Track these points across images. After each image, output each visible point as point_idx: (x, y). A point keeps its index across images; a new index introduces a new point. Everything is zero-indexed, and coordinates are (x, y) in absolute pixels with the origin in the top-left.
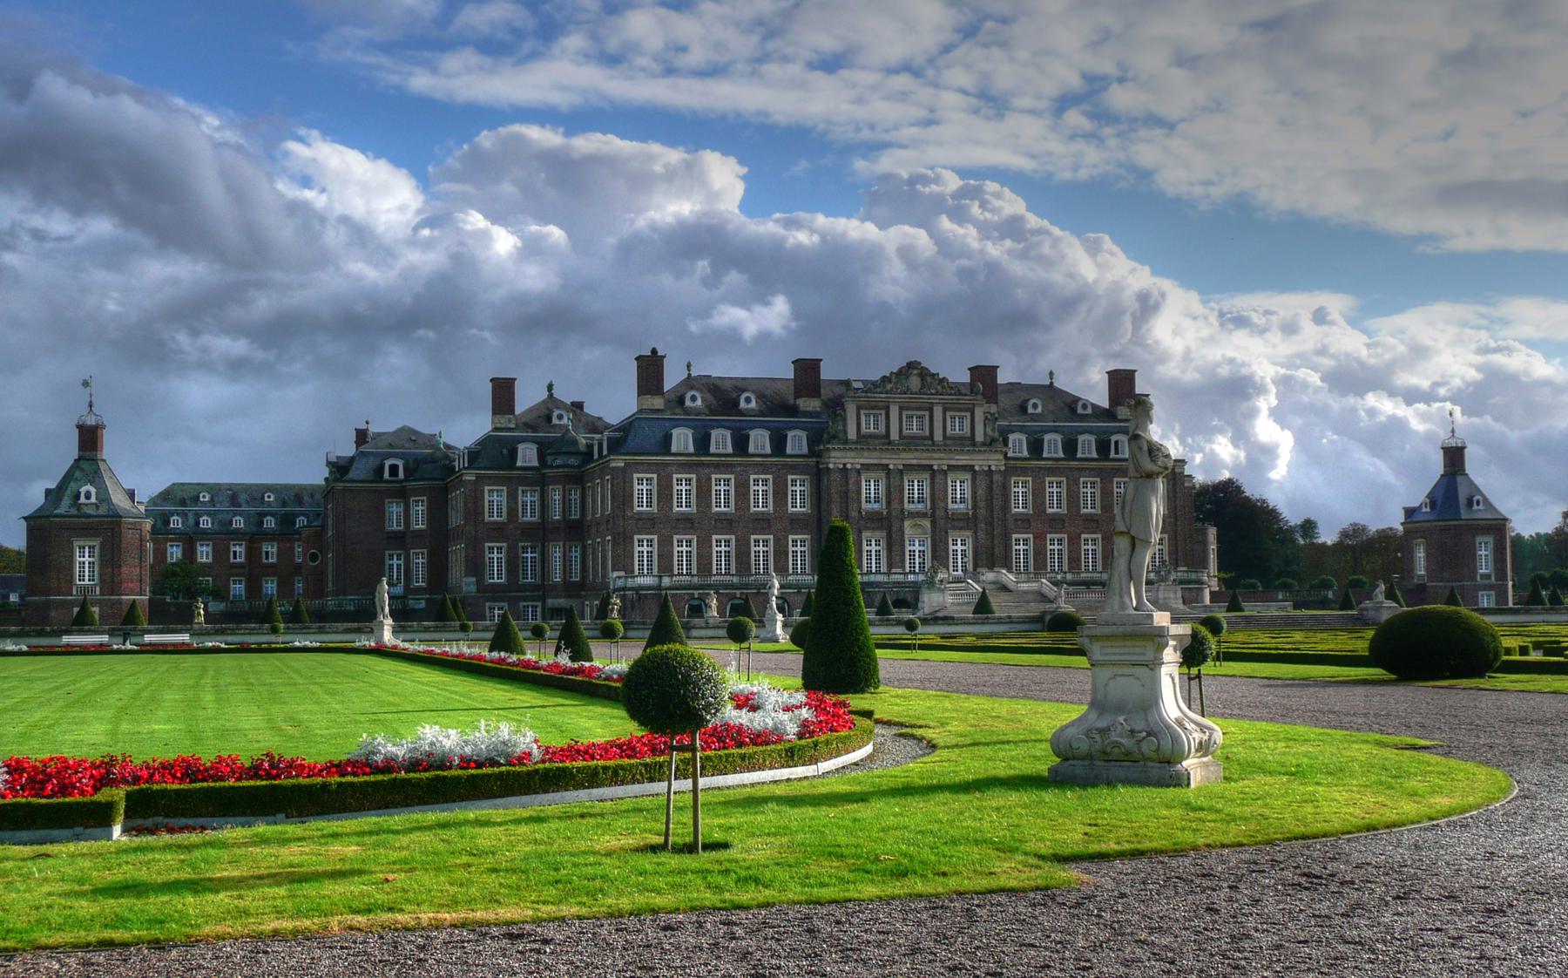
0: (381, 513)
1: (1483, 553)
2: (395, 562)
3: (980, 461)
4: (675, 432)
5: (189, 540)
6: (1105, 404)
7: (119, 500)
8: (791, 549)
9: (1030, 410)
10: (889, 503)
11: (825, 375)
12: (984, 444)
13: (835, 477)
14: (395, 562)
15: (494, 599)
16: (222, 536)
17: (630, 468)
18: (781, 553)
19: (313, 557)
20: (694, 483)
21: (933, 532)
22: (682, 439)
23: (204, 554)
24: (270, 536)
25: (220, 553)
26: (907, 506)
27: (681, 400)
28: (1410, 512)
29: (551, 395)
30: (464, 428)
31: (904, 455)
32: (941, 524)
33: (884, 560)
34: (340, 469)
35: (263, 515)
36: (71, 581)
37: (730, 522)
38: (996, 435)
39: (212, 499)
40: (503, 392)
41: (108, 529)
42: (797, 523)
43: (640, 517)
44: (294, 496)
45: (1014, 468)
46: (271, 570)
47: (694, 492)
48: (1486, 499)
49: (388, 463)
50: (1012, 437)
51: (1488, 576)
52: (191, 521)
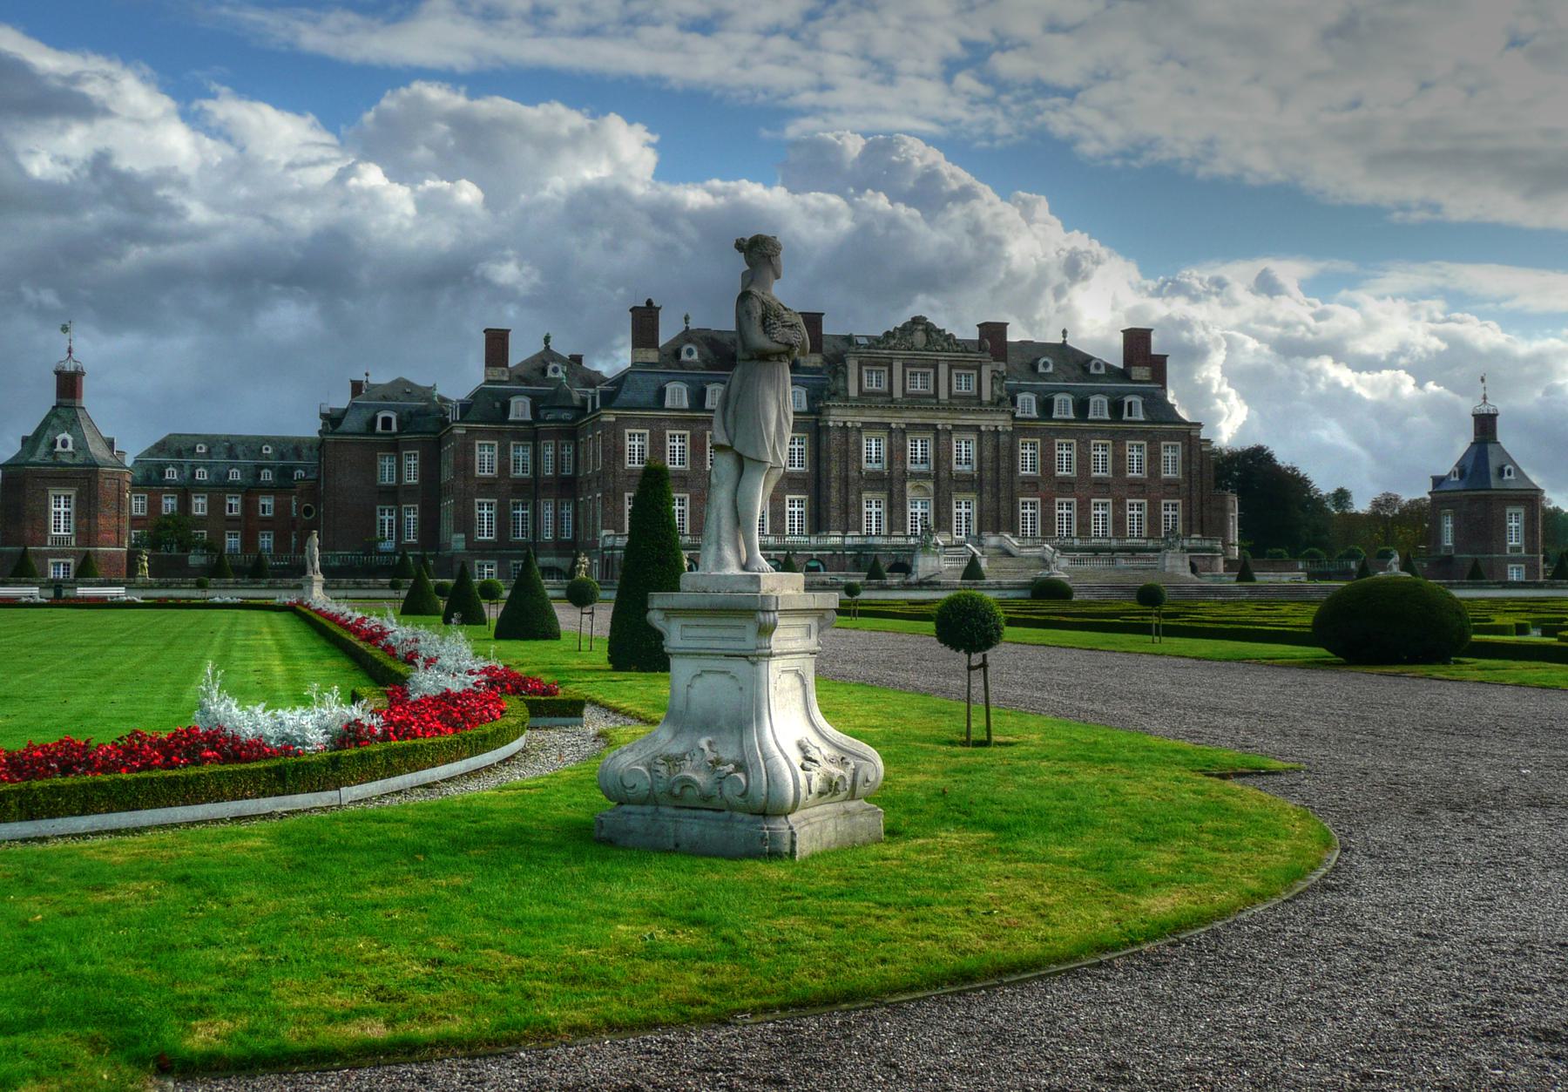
0: (372, 466)
1: (1513, 524)
2: (387, 517)
3: (986, 422)
4: (669, 387)
5: (185, 492)
6: (1119, 363)
7: (98, 451)
8: (788, 509)
9: (1041, 369)
10: (890, 463)
12: (991, 404)
13: (835, 435)
14: (387, 517)
15: (482, 557)
16: (219, 488)
17: (622, 422)
19: (308, 511)
20: (688, 439)
21: (936, 493)
22: (677, 395)
23: (199, 506)
24: (268, 490)
25: (216, 506)
27: (677, 354)
28: (1438, 481)
29: (547, 348)
30: (459, 376)
31: (907, 414)
32: (944, 485)
33: (884, 522)
34: (332, 420)
35: (262, 467)
36: (46, 530)
38: (1004, 394)
39: (209, 451)
40: (497, 343)
41: (85, 479)
44: (291, 448)
45: (1023, 428)
46: (267, 524)
47: (688, 449)
48: (1518, 469)
49: (381, 415)
50: (1020, 397)
51: (1518, 549)
52: (187, 473)
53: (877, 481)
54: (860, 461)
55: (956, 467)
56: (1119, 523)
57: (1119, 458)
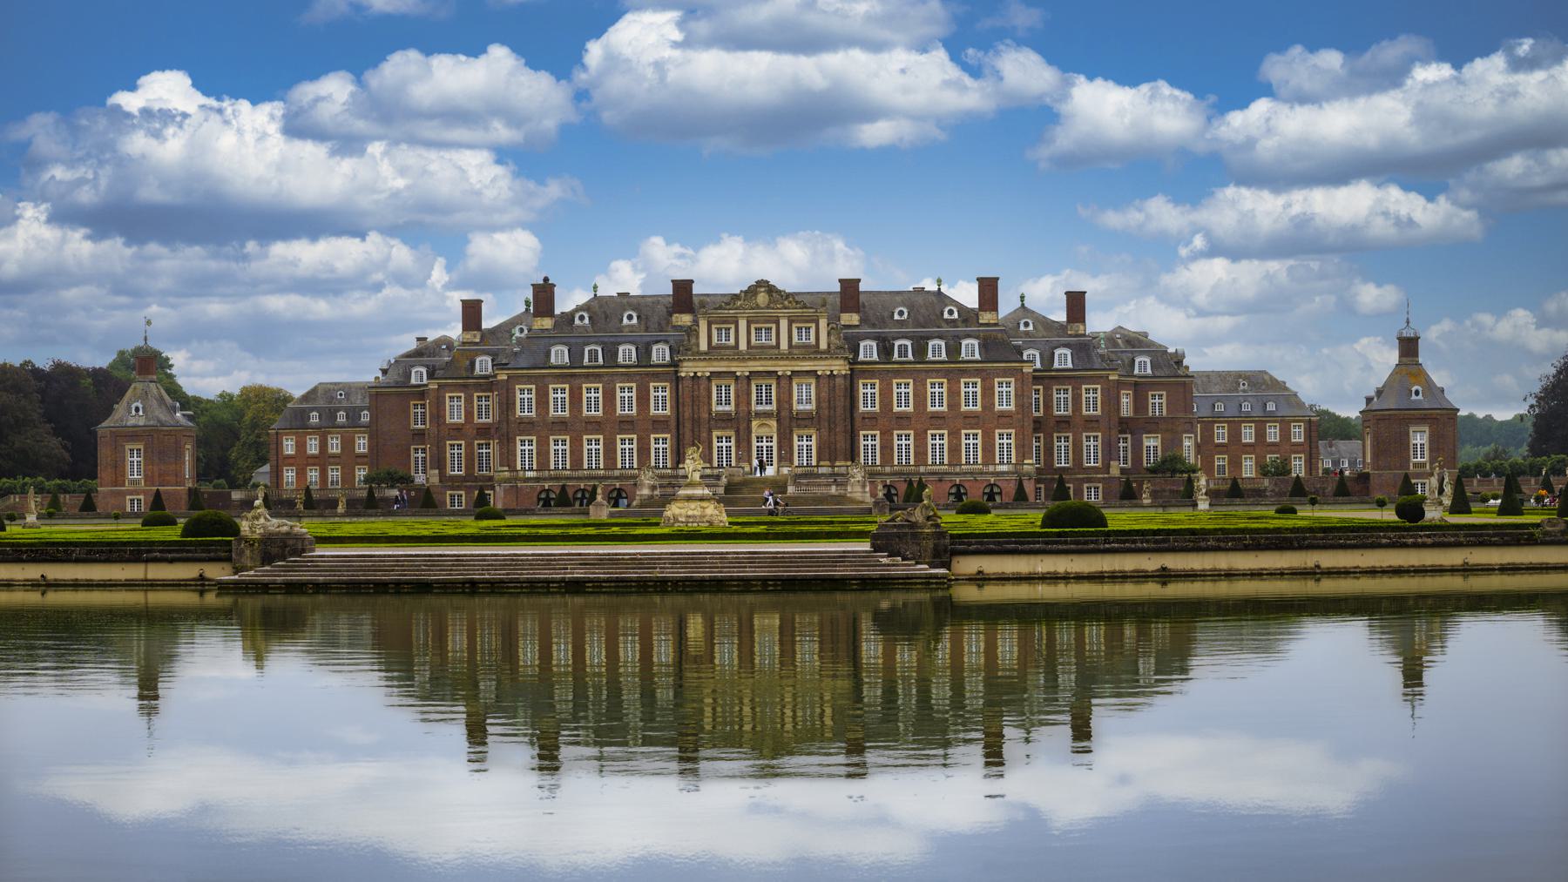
3: (822, 367)
8: (653, 446)
9: (896, 317)
10: (737, 405)
11: (696, 290)
12: (823, 352)
14: (420, 455)
15: (452, 489)
18: (644, 451)
22: (559, 354)
25: (348, 444)
26: (755, 407)
28: (1369, 400)
32: (789, 422)
36: (124, 475)
37: (598, 423)
40: (472, 312)
42: (659, 424)
43: (521, 421)
45: (857, 371)
51: (1423, 465)
53: (725, 420)
54: (710, 404)
55: (796, 407)
56: (955, 450)
57: (954, 393)
